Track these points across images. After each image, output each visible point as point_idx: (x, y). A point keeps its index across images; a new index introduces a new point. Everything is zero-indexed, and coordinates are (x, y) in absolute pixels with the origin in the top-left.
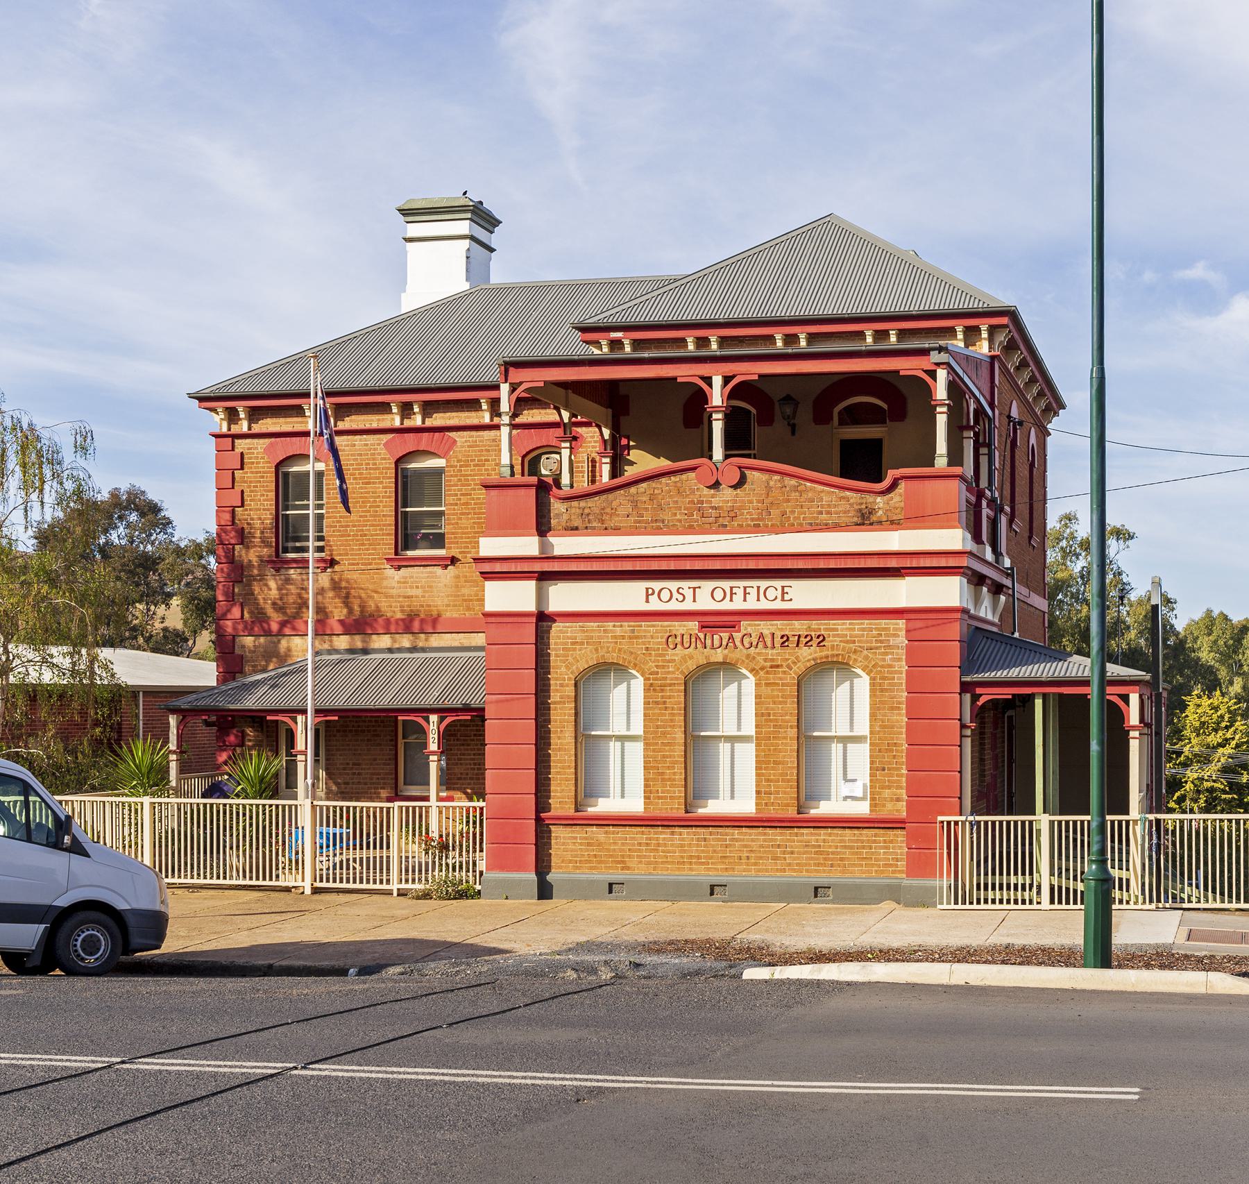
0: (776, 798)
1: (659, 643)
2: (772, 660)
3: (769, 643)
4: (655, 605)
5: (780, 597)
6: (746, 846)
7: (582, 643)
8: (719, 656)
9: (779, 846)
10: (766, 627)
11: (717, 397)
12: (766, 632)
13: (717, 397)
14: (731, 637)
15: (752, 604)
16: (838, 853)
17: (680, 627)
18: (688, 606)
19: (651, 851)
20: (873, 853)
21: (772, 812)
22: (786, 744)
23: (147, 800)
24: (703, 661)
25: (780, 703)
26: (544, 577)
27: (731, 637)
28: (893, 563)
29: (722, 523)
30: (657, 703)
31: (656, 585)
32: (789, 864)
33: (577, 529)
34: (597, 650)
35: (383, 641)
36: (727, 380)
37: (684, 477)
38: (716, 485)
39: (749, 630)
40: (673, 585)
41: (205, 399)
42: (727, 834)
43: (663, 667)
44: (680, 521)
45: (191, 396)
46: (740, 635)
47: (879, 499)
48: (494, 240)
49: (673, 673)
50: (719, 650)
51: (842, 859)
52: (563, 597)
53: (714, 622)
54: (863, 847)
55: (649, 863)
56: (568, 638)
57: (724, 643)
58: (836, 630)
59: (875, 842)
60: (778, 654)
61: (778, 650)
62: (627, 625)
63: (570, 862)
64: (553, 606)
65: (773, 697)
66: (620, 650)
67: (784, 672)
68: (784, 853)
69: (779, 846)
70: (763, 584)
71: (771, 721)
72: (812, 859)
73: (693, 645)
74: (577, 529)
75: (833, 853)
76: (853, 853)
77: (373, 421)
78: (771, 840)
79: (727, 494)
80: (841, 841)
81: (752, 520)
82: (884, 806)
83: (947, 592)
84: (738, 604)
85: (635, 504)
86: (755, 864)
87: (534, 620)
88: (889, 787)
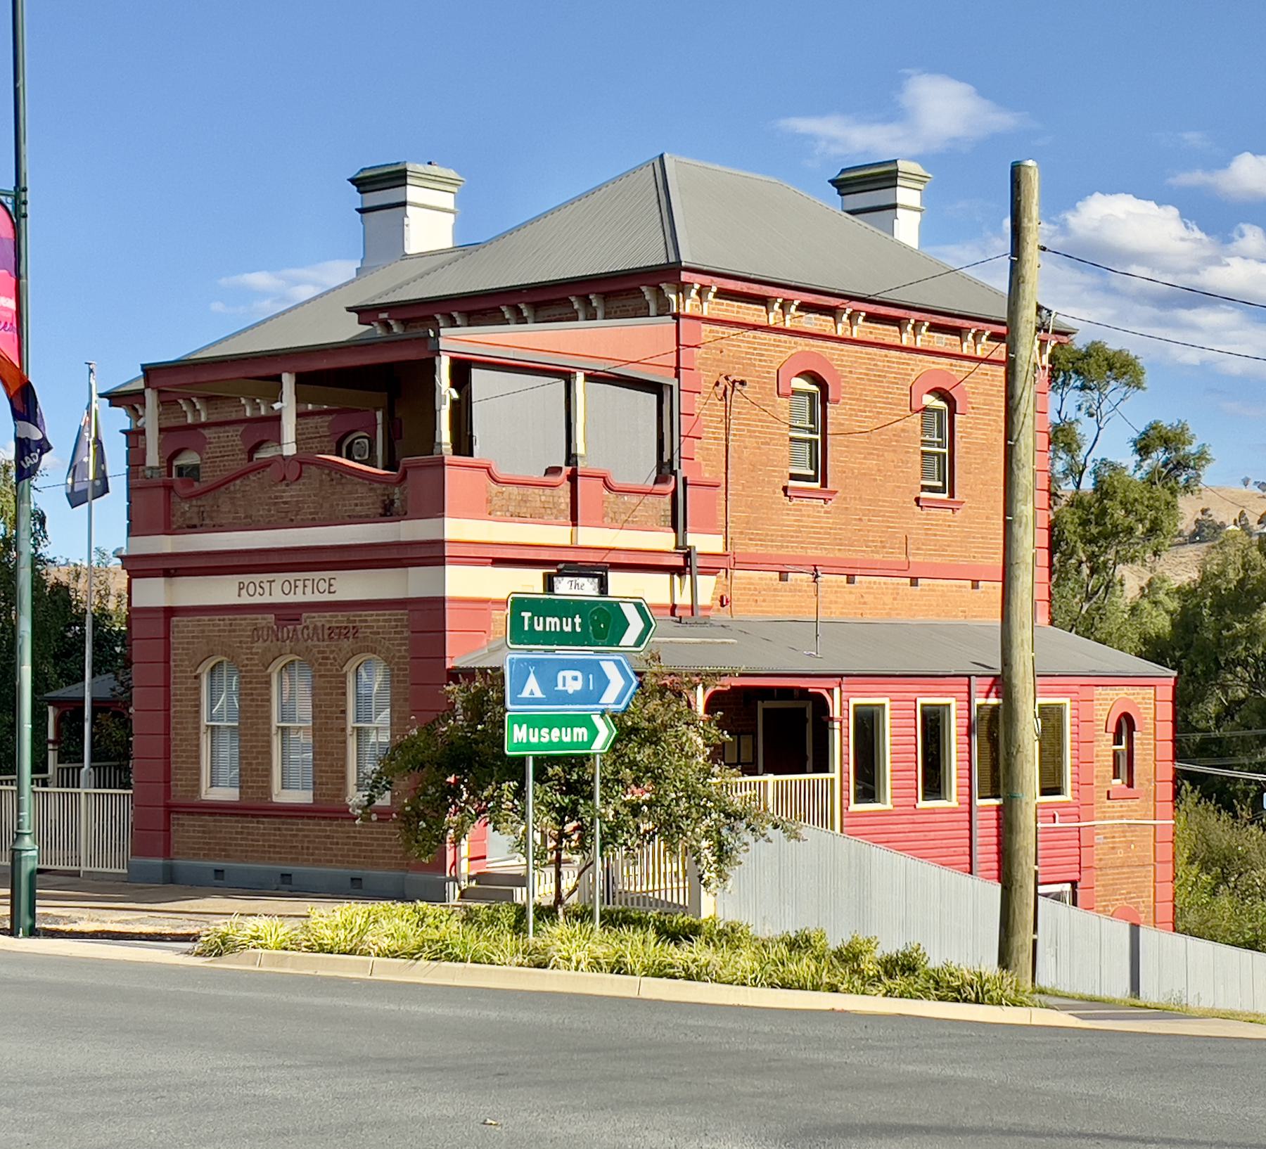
2: (324, 652)
10: (319, 619)
12: (319, 624)
18: (266, 599)
23: (771, 778)
31: (246, 578)
32: (336, 855)
33: (195, 526)
47: (397, 490)
49: (256, 665)
54: (386, 839)
58: (366, 621)
70: (317, 575)
74: (195, 526)
81: (311, 513)
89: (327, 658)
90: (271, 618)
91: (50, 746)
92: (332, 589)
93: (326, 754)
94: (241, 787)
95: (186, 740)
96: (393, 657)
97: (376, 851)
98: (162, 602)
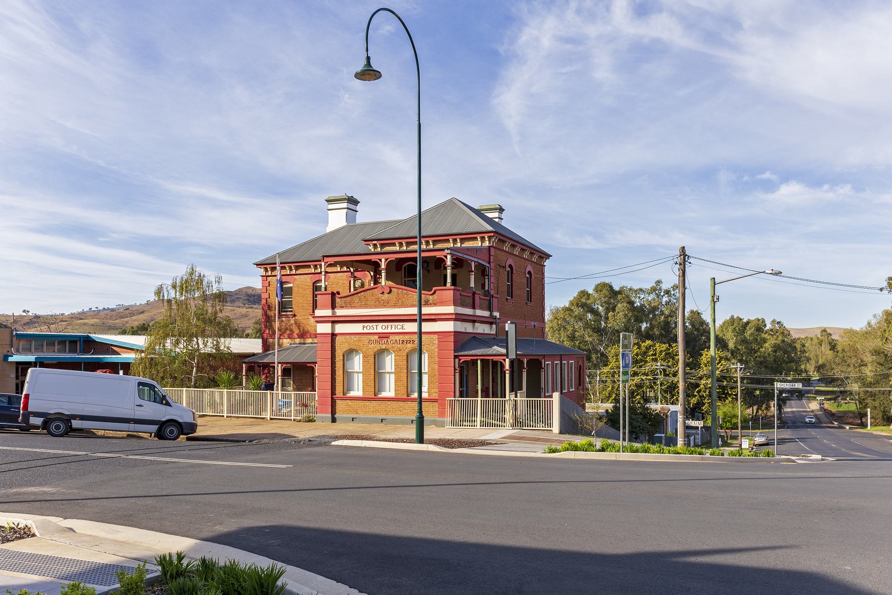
4: (366, 331)
8: (384, 347)
10: (397, 338)
15: (393, 330)
18: (375, 331)
26: (333, 322)
28: (433, 317)
29: (385, 305)
31: (366, 324)
35: (310, 340)
36: (386, 260)
38: (383, 293)
40: (371, 324)
48: (358, 208)
52: (340, 328)
53: (384, 336)
62: (357, 337)
64: (337, 331)
70: (397, 324)
79: (386, 295)
84: (389, 331)
90: (376, 337)
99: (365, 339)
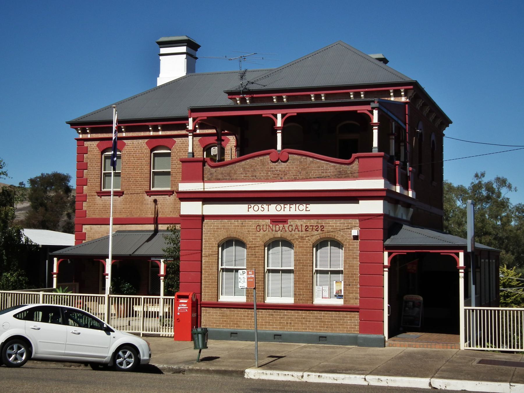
0: (303, 297)
1: (253, 229)
3: (300, 230)
4: (252, 212)
5: (305, 209)
6: (289, 318)
7: (221, 229)
9: (304, 318)
10: (298, 222)
11: (279, 123)
12: (299, 224)
13: (279, 123)
14: (284, 226)
16: (329, 322)
17: (262, 222)
18: (266, 213)
19: (249, 319)
20: (345, 322)
21: (301, 303)
22: (307, 274)
24: (272, 237)
25: (305, 255)
27: (284, 226)
30: (252, 255)
32: (308, 327)
34: (227, 231)
36: (283, 116)
37: (265, 157)
39: (292, 223)
41: (73, 124)
42: (282, 313)
43: (255, 239)
44: (263, 176)
45: (68, 123)
46: (288, 225)
50: (279, 232)
51: (331, 325)
53: (277, 219)
54: (341, 320)
55: (247, 325)
56: (215, 226)
57: (281, 229)
58: (329, 223)
59: (346, 317)
60: (304, 234)
61: (304, 232)
63: (215, 323)
65: (302, 253)
66: (237, 231)
67: (307, 242)
68: (306, 321)
69: (304, 318)
71: (301, 263)
72: (318, 324)
73: (267, 230)
74: (219, 179)
75: (327, 322)
76: (335, 322)
77: (142, 134)
78: (300, 316)
80: (331, 317)
81: (294, 176)
82: (350, 301)
83: (376, 207)
85: (244, 168)
86: (294, 326)
87: (201, 218)
88: (352, 293)
89: (304, 239)
90: (268, 221)
91: (55, 276)
92: (307, 209)
93: (303, 281)
94: (247, 296)
95: (211, 274)
96: (346, 239)
97: (334, 325)
98: (200, 213)
99: (252, 223)
